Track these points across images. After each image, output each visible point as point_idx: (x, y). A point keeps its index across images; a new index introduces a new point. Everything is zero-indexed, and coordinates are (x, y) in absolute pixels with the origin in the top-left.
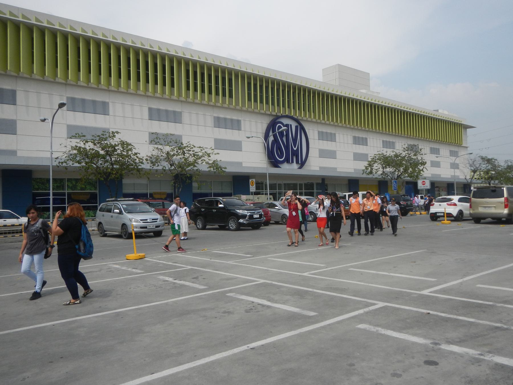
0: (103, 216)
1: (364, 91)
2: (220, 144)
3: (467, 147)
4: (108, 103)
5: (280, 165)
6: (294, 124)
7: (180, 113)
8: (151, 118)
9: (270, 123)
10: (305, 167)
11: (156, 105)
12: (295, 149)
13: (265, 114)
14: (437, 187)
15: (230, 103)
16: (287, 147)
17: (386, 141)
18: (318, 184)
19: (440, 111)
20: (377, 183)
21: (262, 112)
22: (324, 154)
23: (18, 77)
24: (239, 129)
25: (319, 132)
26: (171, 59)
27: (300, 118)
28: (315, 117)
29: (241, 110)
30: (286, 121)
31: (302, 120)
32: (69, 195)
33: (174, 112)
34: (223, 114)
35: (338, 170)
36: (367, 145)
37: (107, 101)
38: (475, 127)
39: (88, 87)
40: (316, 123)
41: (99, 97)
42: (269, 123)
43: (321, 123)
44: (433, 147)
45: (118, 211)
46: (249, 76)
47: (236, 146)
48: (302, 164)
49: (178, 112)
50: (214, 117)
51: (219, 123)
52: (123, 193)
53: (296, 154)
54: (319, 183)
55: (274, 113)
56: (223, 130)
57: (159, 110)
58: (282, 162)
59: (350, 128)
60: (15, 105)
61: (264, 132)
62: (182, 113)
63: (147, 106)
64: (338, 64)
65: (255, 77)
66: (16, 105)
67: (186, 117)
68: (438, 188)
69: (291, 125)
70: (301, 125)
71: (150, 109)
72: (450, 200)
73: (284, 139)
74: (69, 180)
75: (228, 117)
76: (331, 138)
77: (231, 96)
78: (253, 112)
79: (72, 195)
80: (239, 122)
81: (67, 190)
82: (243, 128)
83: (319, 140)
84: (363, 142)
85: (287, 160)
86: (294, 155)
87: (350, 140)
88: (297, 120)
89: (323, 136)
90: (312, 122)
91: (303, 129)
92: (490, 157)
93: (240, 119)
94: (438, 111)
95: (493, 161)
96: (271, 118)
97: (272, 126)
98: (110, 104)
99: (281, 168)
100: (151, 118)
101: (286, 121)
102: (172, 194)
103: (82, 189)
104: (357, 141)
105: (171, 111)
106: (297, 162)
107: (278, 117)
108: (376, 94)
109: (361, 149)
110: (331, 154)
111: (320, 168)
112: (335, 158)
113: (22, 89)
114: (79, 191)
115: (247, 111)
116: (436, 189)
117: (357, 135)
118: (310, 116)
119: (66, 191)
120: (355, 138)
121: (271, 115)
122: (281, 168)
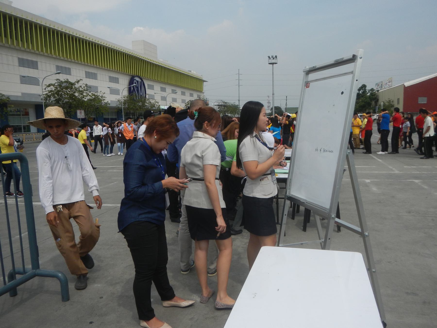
3: (204, 93)
12: (141, 94)
17: (173, 89)
19: (192, 72)
27: (141, 77)
30: (137, 79)
33: (95, 74)
37: (70, 67)
42: (130, 79)
50: (109, 76)
55: (131, 75)
64: (144, 41)
67: (99, 76)
70: (142, 80)
71: (86, 72)
75: (114, 76)
76: (151, 87)
80: (118, 78)
88: (141, 79)
90: (145, 79)
92: (225, 101)
93: (118, 77)
94: (191, 71)
95: (227, 103)
102: (95, 118)
108: (166, 62)
117: (162, 86)
120: (161, 88)
121: (130, 75)
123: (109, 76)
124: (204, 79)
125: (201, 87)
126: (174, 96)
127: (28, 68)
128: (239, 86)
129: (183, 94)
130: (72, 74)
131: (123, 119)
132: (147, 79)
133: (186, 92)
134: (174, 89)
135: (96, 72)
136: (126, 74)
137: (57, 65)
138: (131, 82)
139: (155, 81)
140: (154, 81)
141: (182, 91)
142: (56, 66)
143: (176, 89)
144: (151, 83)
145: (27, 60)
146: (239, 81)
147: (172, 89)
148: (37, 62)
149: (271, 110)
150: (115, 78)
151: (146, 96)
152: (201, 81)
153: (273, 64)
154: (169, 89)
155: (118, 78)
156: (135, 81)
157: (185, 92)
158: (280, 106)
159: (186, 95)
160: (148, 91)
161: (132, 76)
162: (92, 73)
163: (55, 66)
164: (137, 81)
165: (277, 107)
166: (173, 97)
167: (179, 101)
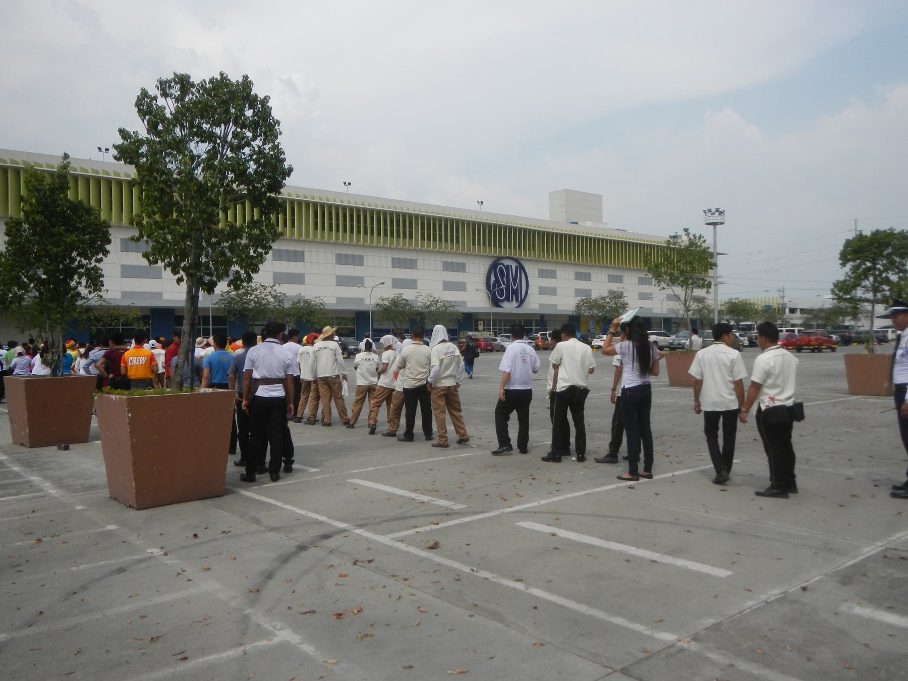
1: (589, 224)
2: (448, 286)
5: (502, 304)
6: (514, 265)
7: (416, 260)
8: (393, 267)
9: (492, 264)
10: (525, 305)
11: (397, 255)
12: (515, 288)
13: (487, 256)
14: (675, 323)
15: (458, 248)
16: (507, 288)
17: (613, 275)
18: (536, 321)
21: (485, 254)
22: (543, 291)
23: (306, 241)
24: (464, 271)
25: (539, 270)
26: (410, 216)
27: (520, 258)
28: (535, 256)
29: (466, 255)
31: (522, 259)
33: (411, 260)
34: (450, 259)
35: (559, 308)
36: (590, 280)
37: (362, 254)
39: (350, 245)
40: (537, 261)
41: (357, 252)
42: (491, 264)
43: (541, 261)
46: (474, 223)
47: (460, 287)
48: (521, 302)
49: (414, 259)
50: (444, 262)
51: (448, 267)
53: (515, 292)
54: (538, 320)
55: (495, 255)
56: (450, 273)
57: (399, 259)
58: (503, 301)
59: (571, 264)
61: (487, 273)
65: (479, 224)
67: (420, 263)
68: (676, 325)
69: (511, 266)
71: (393, 259)
72: (602, 338)
73: (505, 279)
74: (337, 318)
76: (552, 275)
77: (458, 242)
78: (477, 255)
80: (464, 264)
82: (467, 271)
83: (539, 277)
84: (587, 277)
85: (507, 299)
86: (514, 294)
89: (542, 274)
90: (531, 260)
91: (522, 268)
93: (465, 262)
97: (493, 267)
98: (364, 256)
99: (503, 307)
100: (393, 267)
101: (506, 262)
102: (409, 330)
103: (345, 325)
104: (579, 276)
105: (408, 259)
106: (517, 300)
107: (499, 258)
109: (583, 285)
110: (552, 291)
111: (540, 305)
112: (555, 294)
115: (471, 255)
116: (673, 325)
117: (579, 271)
118: (530, 255)
120: (577, 273)
121: (493, 257)
122: (503, 307)
123: (444, 262)
127: (288, 261)
130: (365, 263)
134: (614, 274)
135: (414, 258)
136: (482, 256)
137: (338, 252)
142: (336, 254)
143: (622, 274)
145: (287, 251)
147: (611, 273)
148: (303, 253)
150: (458, 264)
153: (715, 224)
155: (464, 264)
162: (405, 260)
163: (334, 255)
164: (507, 267)
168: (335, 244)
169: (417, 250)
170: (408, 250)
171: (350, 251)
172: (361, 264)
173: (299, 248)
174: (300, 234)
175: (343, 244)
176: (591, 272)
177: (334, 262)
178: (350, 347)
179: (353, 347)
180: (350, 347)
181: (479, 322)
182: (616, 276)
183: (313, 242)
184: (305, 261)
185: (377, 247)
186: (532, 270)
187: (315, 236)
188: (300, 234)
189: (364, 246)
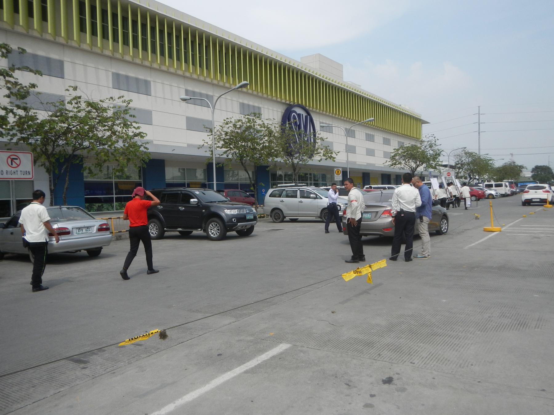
0: (282, 201)
4: (150, 82)
6: (304, 114)
9: (285, 111)
11: (192, 87)
13: (281, 103)
17: (368, 134)
20: (361, 175)
27: (307, 108)
29: (262, 98)
30: (299, 111)
32: (116, 184)
37: (149, 79)
38: (428, 123)
41: (142, 75)
42: (284, 111)
44: (399, 141)
45: (314, 196)
50: (240, 103)
52: (166, 182)
55: (288, 102)
60: (63, 78)
62: (214, 97)
63: (183, 87)
66: (63, 78)
69: (302, 115)
70: (308, 114)
75: (251, 103)
76: (328, 129)
78: (271, 100)
79: (119, 185)
81: (115, 179)
87: (343, 133)
93: (260, 106)
94: (401, 105)
95: (474, 154)
96: (285, 107)
98: (152, 83)
109: (351, 141)
113: (69, 60)
114: (125, 179)
115: (267, 99)
119: (114, 180)
123: (240, 103)
124: (422, 118)
125: (419, 131)
126: (370, 145)
128: (479, 133)
129: (387, 142)
130: (153, 93)
131: (215, 182)
132: (319, 113)
133: (391, 140)
137: (114, 71)
138: (286, 117)
139: (335, 118)
140: (332, 117)
141: (384, 137)
144: (327, 121)
146: (479, 124)
147: (367, 132)
149: (532, 172)
151: (315, 142)
152: (419, 122)
154: (361, 133)
156: (294, 114)
157: (389, 140)
158: (548, 165)
159: (391, 145)
160: (321, 134)
161: (289, 105)
163: (110, 74)
164: (299, 115)
165: (544, 166)
166: (367, 147)
167: (379, 154)
168: (111, 58)
169: (213, 85)
170: (204, 82)
171: (132, 73)
172: (148, 93)
173: (54, 54)
174: (56, 30)
175: (122, 61)
176: (355, 129)
177: (111, 86)
178: (228, 212)
179: (235, 212)
180: (228, 212)
181: (335, 170)
182: (370, 135)
183: (79, 49)
184: (66, 76)
185: (168, 72)
186: (318, 121)
187: (82, 40)
188: (56, 30)
189: (151, 68)
